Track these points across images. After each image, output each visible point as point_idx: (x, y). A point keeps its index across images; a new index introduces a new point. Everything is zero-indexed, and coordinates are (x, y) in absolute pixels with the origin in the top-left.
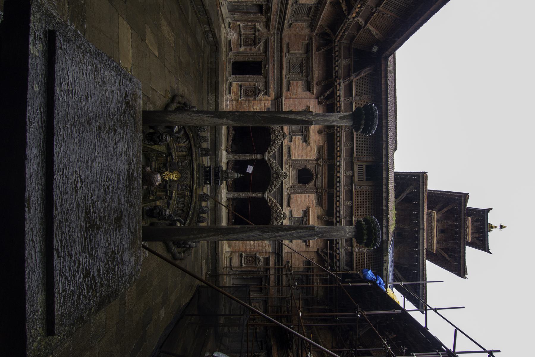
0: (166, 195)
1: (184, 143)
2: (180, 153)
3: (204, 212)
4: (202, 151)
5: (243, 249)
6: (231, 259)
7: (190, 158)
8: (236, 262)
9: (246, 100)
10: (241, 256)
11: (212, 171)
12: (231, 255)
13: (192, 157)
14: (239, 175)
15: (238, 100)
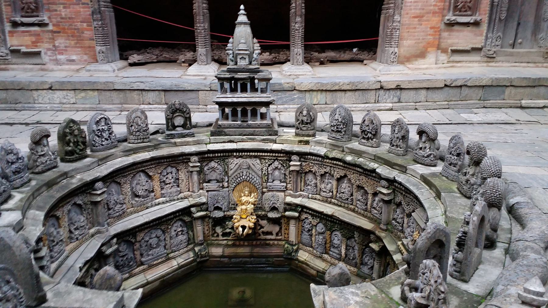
0: (297, 219)
1: (150, 177)
2: (183, 185)
3: (347, 122)
4: (174, 127)
5: (435, 20)
6: (454, 52)
7: (195, 158)
8: (464, 38)
9: (49, 10)
10: (451, 25)
11: (230, 98)
12: (444, 51)
13: (191, 154)
14: (242, 18)
15: (52, 32)
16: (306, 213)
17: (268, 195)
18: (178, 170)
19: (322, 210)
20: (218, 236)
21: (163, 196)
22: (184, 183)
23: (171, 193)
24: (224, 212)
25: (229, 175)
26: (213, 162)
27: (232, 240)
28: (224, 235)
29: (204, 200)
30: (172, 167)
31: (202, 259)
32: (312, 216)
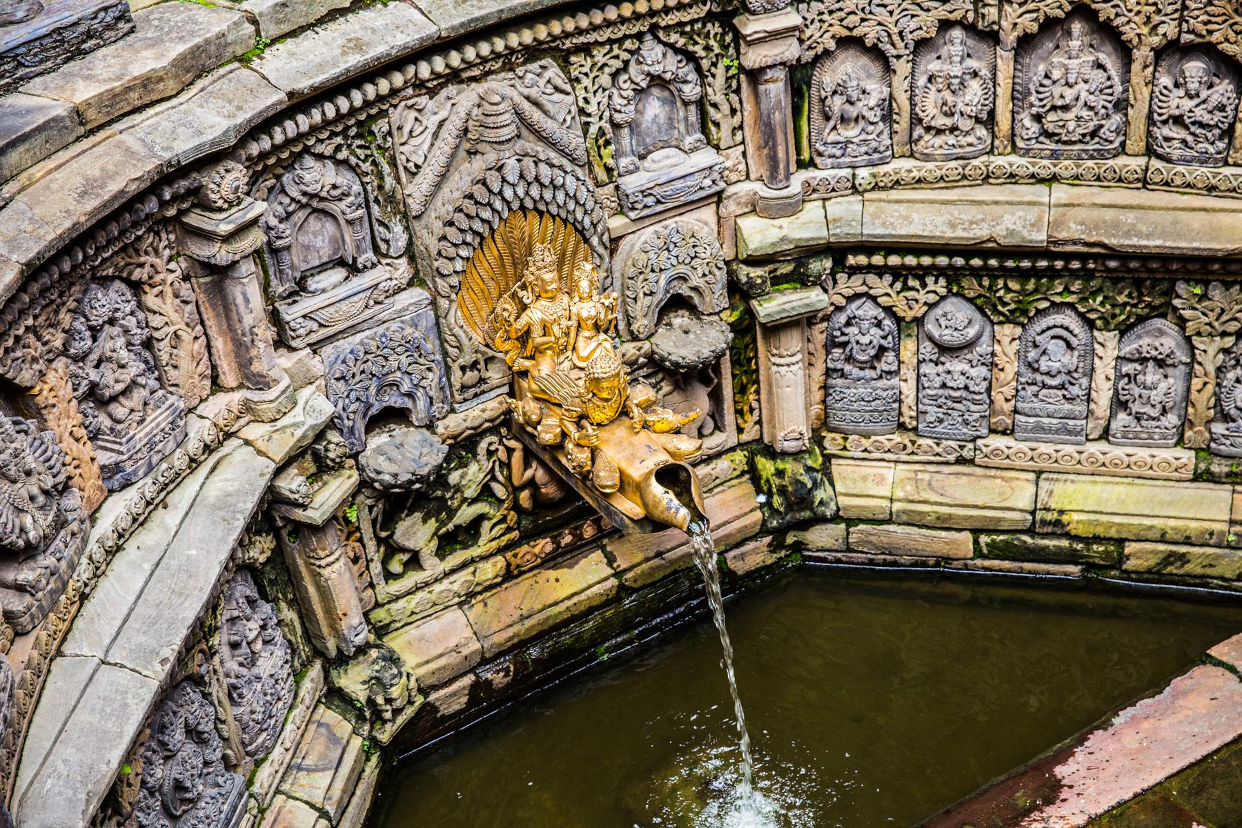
13: (211, 159)
16: (854, 271)
17: (641, 242)
18: (137, 287)
19: (981, 232)
20: (414, 561)
21: (115, 478)
22: (183, 354)
23: (151, 445)
24: (430, 427)
25: (415, 206)
26: (309, 161)
27: (501, 551)
28: (447, 542)
29: (326, 409)
30: (105, 282)
31: (401, 720)
32: (898, 273)
